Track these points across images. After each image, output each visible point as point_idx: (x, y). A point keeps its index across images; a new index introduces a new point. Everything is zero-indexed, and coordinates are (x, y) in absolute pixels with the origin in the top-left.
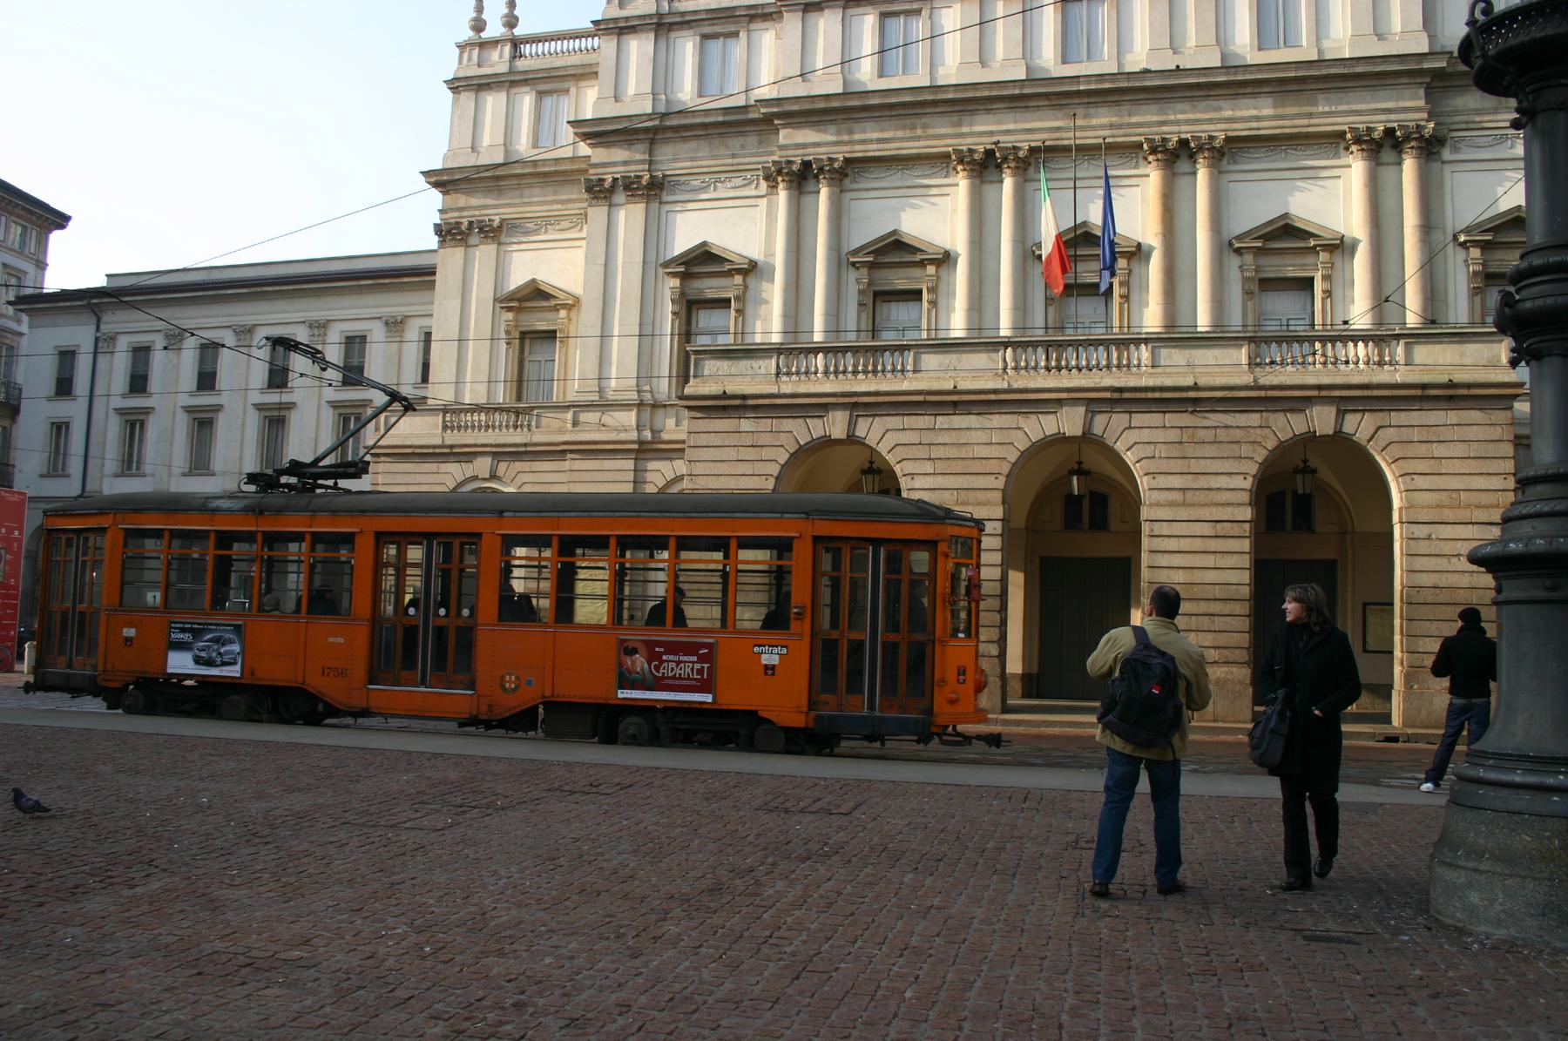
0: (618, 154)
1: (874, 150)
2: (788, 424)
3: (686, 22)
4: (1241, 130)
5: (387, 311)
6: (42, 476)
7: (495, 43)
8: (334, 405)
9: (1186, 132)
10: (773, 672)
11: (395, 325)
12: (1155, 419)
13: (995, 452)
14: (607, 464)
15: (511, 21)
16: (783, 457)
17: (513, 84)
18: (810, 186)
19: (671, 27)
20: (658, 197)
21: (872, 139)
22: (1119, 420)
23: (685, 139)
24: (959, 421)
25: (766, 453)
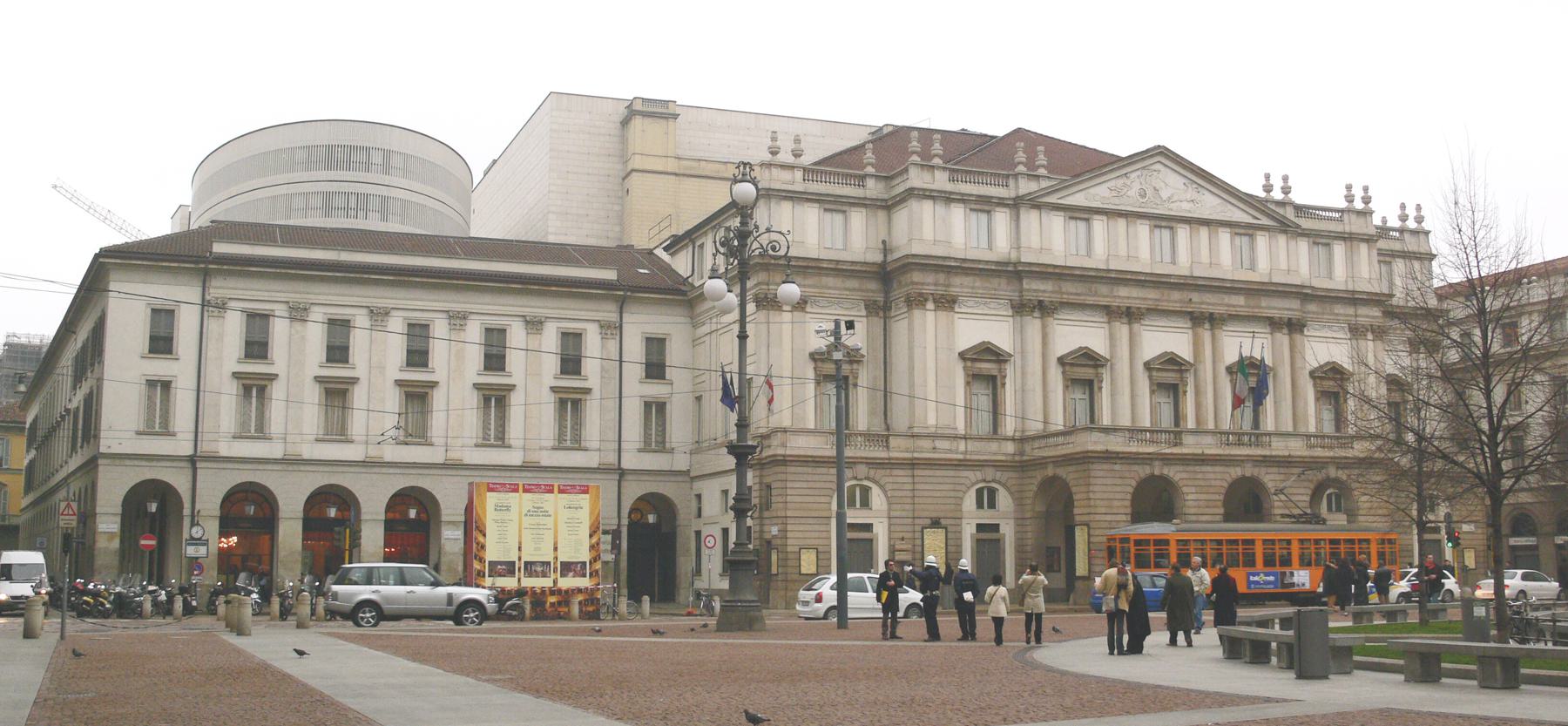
0: (930, 278)
1: (1072, 299)
2: (1136, 468)
3: (963, 199)
4: (1233, 311)
5: (526, 311)
6: (139, 433)
7: (792, 167)
8: (477, 386)
9: (1211, 309)
10: (491, 607)
11: (534, 325)
12: (1274, 470)
13: (1218, 483)
14: (938, 473)
15: (797, 154)
16: (1134, 483)
17: (808, 200)
18: (1036, 314)
19: (954, 200)
20: (952, 309)
21: (1070, 289)
22: (1263, 470)
23: (967, 275)
24: (1205, 469)
25: (1128, 481)
